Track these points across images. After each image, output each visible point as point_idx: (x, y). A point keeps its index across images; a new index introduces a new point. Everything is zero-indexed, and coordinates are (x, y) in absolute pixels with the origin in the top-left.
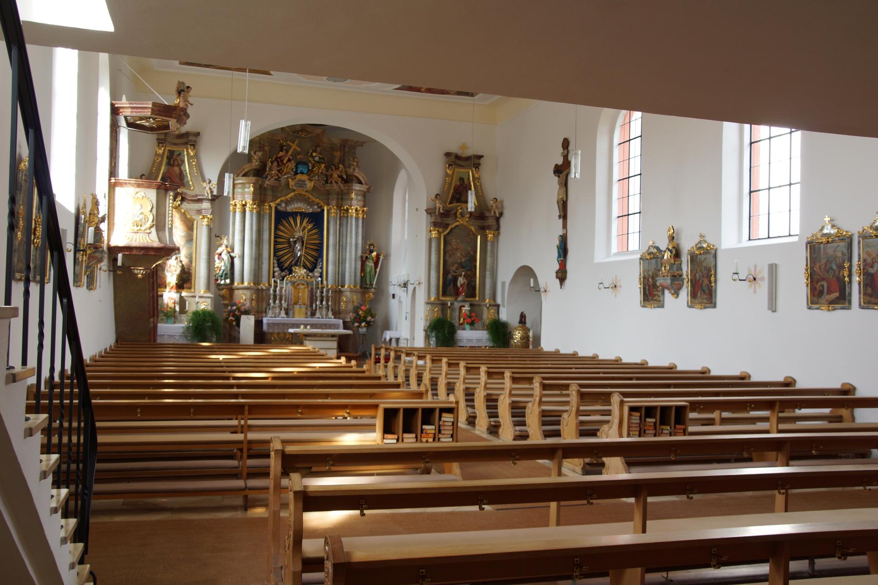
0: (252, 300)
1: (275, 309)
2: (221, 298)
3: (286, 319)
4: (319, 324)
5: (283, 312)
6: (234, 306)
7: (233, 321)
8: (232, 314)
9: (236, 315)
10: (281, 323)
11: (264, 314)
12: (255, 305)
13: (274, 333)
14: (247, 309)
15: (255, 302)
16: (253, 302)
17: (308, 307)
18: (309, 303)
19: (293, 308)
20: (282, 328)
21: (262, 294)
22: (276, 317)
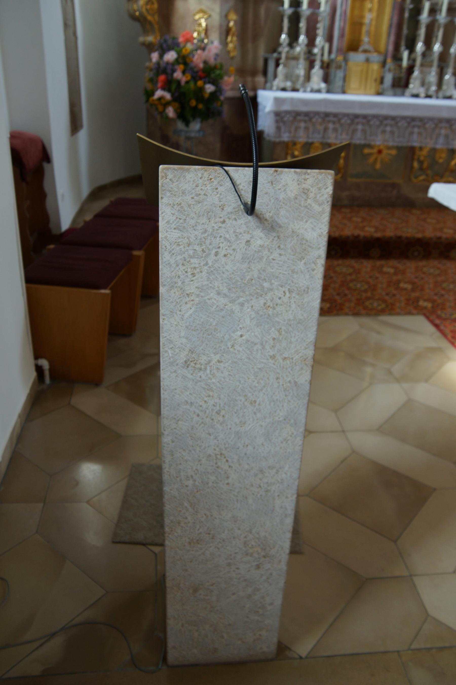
0: (228, 31)
1: (293, 63)
2: (137, 25)
3: (323, 96)
4: (431, 119)
5: (317, 72)
6: (169, 49)
7: (167, 104)
8: (162, 78)
9: (178, 82)
10: (317, 113)
11: (260, 79)
12: (235, 48)
13: (295, 144)
14: (212, 62)
15: (235, 39)
16: (229, 39)
17: (389, 60)
18: (391, 48)
19: (346, 60)
20: (321, 128)
21: (256, 16)
22: (295, 90)
